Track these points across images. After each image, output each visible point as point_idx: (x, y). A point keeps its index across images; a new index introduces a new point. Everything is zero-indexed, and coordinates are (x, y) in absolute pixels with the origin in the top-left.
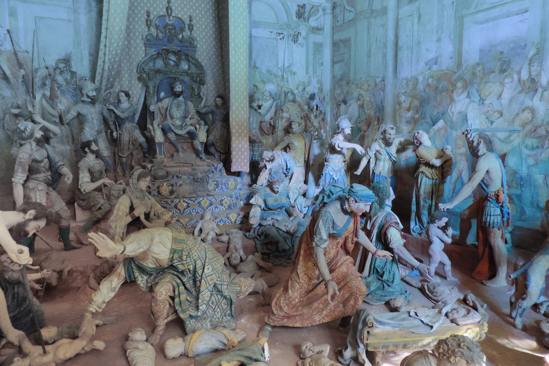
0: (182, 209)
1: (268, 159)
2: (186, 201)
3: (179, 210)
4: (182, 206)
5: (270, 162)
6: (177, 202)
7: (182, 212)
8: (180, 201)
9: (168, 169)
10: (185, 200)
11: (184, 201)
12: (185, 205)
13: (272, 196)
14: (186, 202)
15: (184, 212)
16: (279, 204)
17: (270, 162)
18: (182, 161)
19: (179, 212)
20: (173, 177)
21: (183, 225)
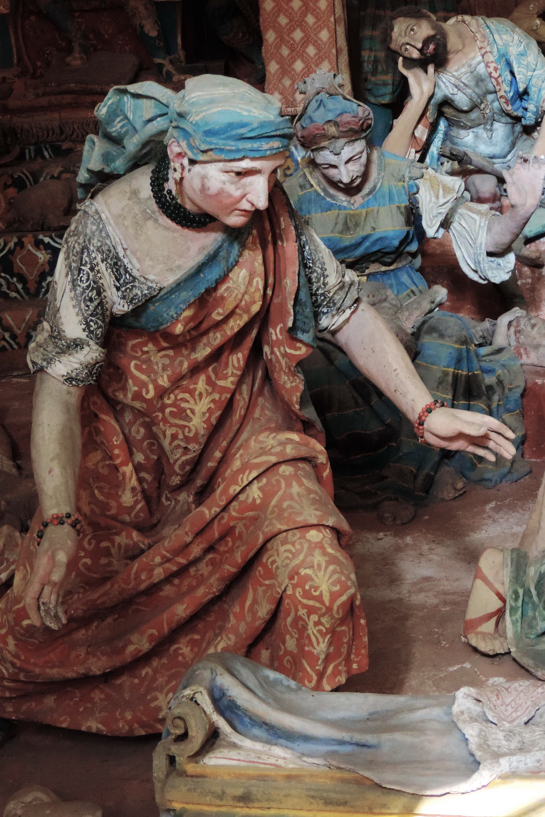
0: (32, 276)
1: (415, 54)
2: (47, 240)
3: (22, 279)
4: (32, 260)
5: (431, 69)
6: (11, 245)
7: (32, 287)
8: (20, 244)
9: (19, 121)
10: (41, 237)
11: (38, 244)
12: (42, 256)
13: (330, 207)
14: (48, 246)
15: (40, 287)
16: (365, 238)
17: (431, 69)
18: (72, 85)
19: (20, 286)
20: (39, 153)
21: (14, 337)
